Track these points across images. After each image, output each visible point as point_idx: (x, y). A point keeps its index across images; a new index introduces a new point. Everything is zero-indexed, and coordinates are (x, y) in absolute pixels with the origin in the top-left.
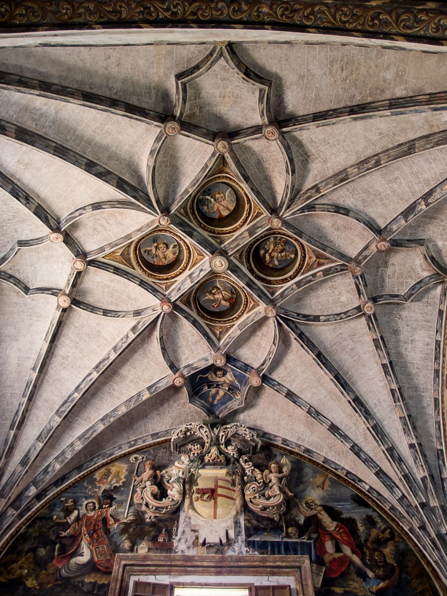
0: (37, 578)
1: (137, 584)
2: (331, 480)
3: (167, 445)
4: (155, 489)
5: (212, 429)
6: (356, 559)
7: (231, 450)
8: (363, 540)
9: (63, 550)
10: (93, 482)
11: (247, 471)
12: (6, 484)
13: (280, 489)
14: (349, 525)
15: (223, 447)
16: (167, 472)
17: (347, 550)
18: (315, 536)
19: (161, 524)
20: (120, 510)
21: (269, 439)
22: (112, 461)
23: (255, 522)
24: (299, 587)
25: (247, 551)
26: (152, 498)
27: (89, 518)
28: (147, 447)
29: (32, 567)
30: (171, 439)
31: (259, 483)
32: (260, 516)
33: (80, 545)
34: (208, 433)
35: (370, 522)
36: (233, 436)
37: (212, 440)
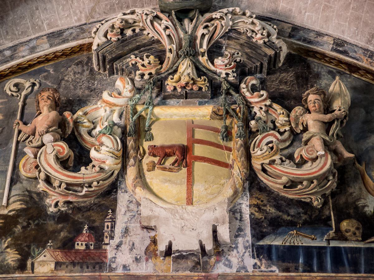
3: (83, 57)
4: (64, 148)
5: (180, 20)
11: (256, 109)
13: (326, 144)
15: (204, 60)
16: (86, 114)
19: (78, 217)
21: (305, 40)
23: (271, 210)
25: (255, 266)
26: (57, 167)
28: (39, 63)
30: (91, 44)
31: (281, 134)
32: (283, 198)
36: (226, 36)
37: (180, 47)
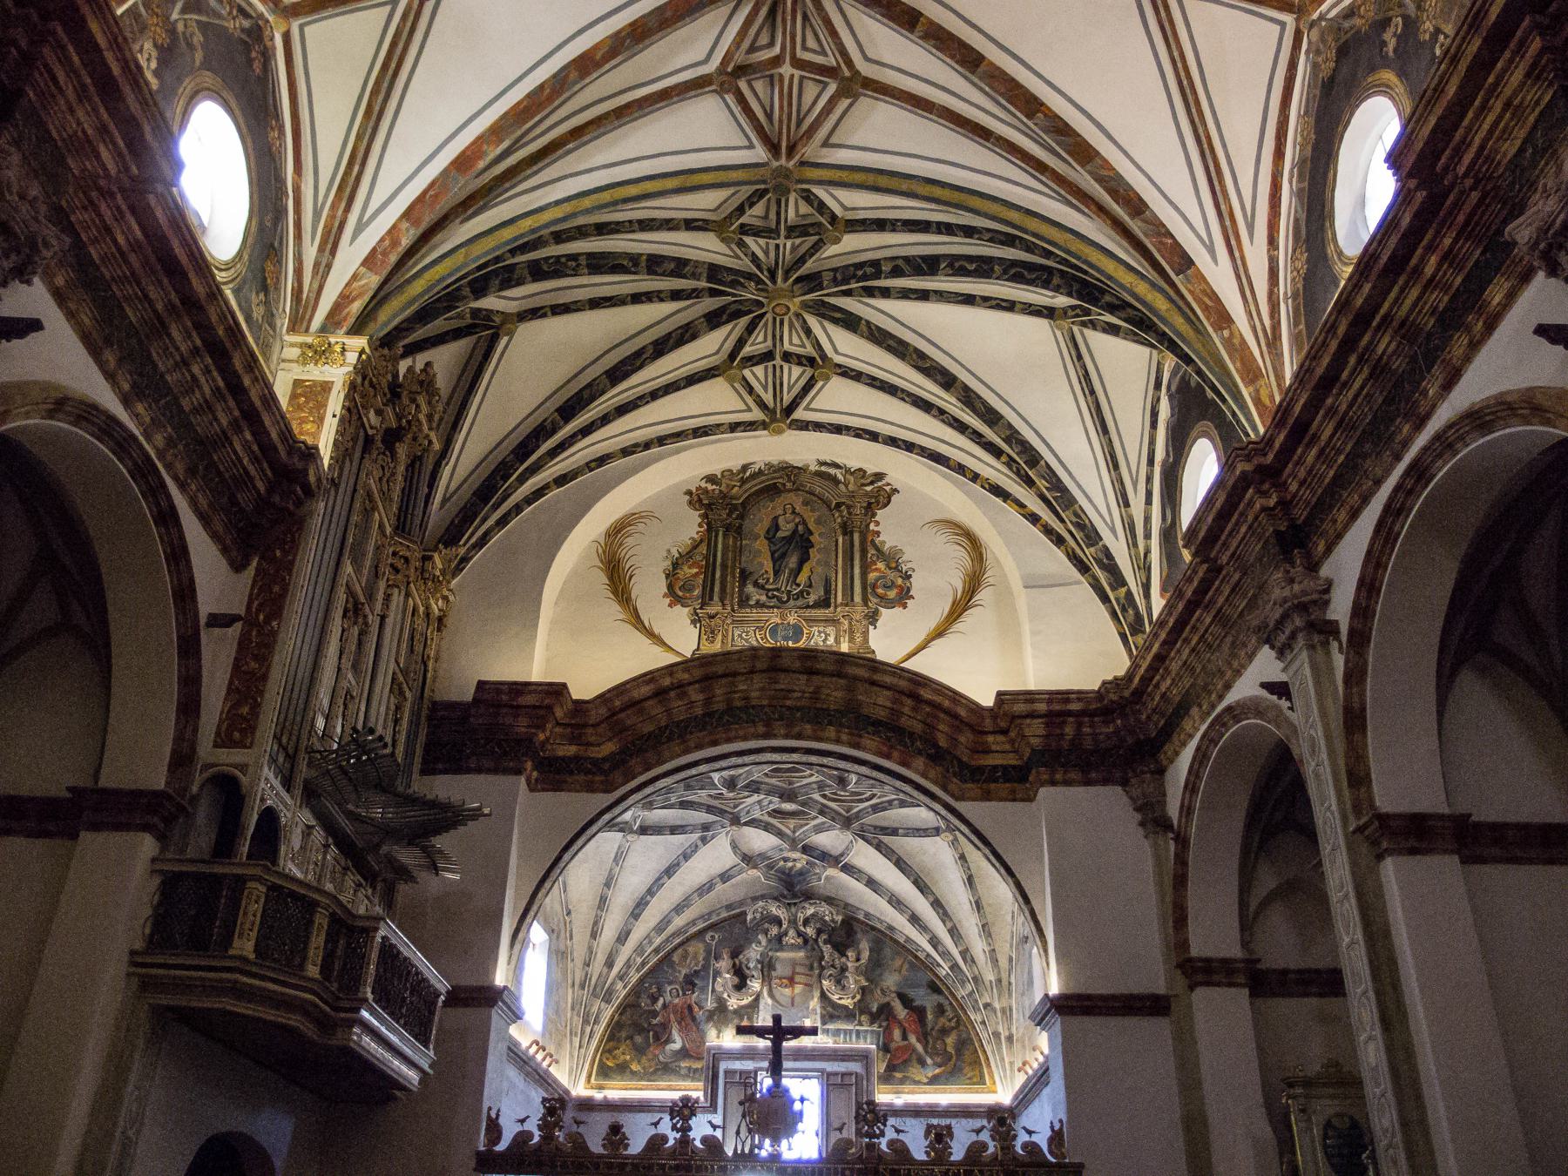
1: (726, 1072)
2: (911, 963)
4: (736, 980)
6: (919, 1047)
7: (810, 931)
9: (657, 1038)
10: (672, 965)
14: (920, 1013)
15: (802, 928)
17: (913, 1039)
18: (884, 1024)
19: (743, 1012)
22: (688, 940)
23: (829, 1009)
29: (634, 1052)
33: (670, 1033)
34: (786, 915)
35: (940, 1011)
36: (813, 915)
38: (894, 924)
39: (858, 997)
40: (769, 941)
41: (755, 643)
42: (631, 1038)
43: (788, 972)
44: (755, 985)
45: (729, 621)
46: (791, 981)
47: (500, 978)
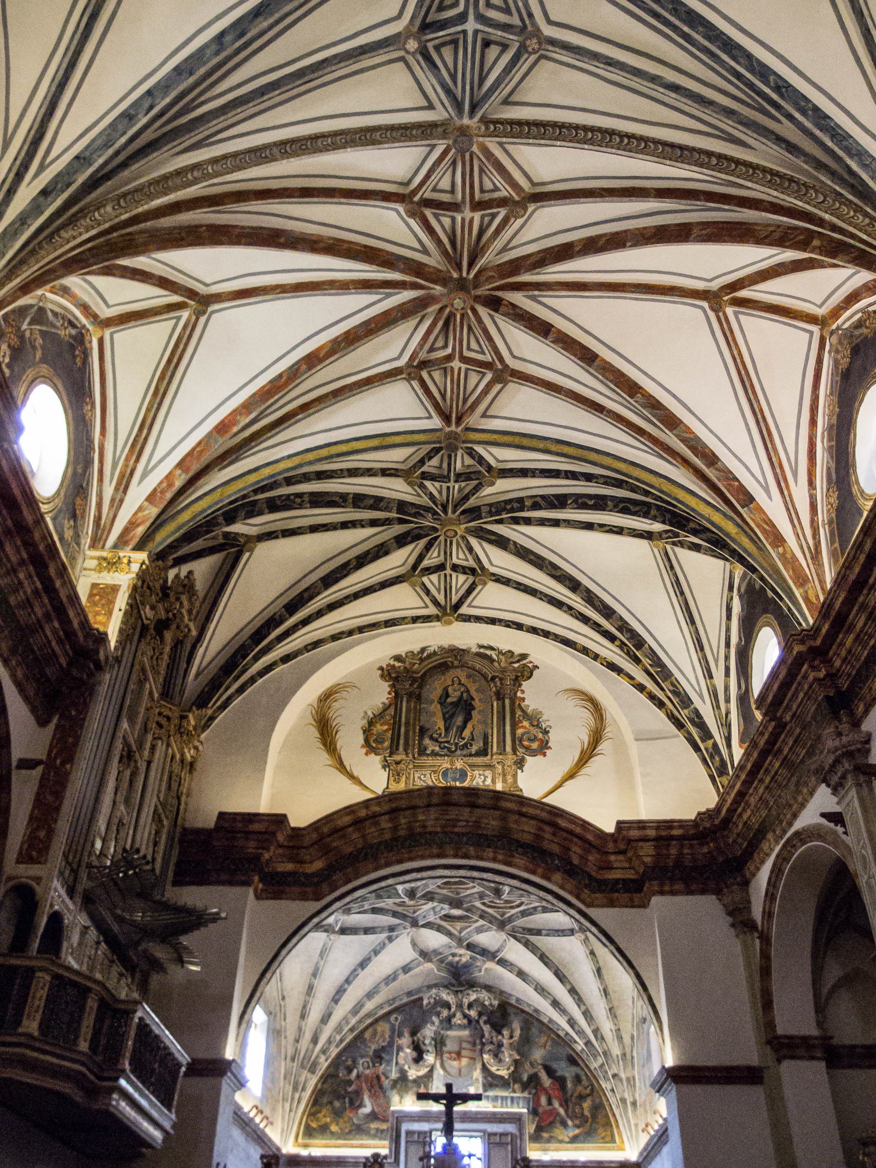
0: (337, 1124)
1: (409, 1133)
3: (418, 1003)
4: (415, 1054)
6: (562, 1111)
7: (473, 1013)
8: (569, 1095)
9: (352, 1103)
10: (364, 1041)
12: (304, 1058)
14: (560, 1081)
15: (467, 1011)
17: (556, 1104)
18: (534, 1091)
20: (389, 1068)
22: (376, 1021)
23: (490, 1079)
24: (518, 1133)
27: (366, 1076)
29: (332, 1116)
33: (362, 1099)
35: (578, 1079)
36: (475, 1000)
38: (539, 1008)
39: (512, 1068)
40: (441, 1022)
41: (430, 783)
42: (331, 1103)
43: (455, 1048)
44: (430, 1058)
45: (411, 766)
46: (459, 1055)
47: (229, 1053)
